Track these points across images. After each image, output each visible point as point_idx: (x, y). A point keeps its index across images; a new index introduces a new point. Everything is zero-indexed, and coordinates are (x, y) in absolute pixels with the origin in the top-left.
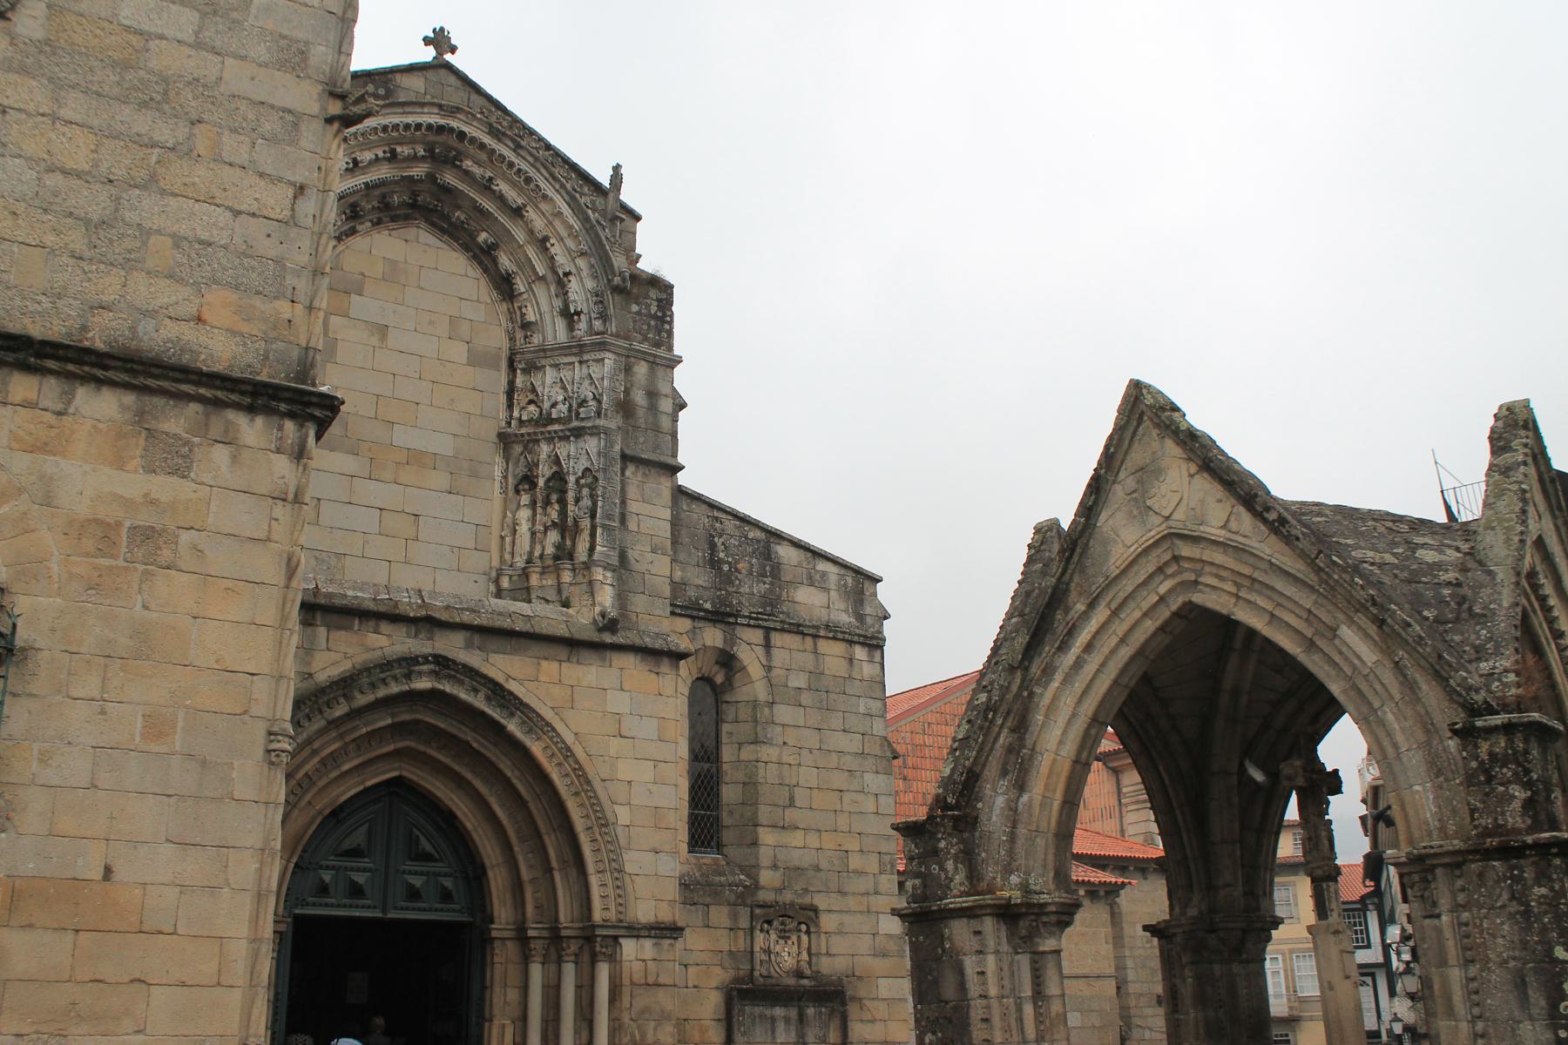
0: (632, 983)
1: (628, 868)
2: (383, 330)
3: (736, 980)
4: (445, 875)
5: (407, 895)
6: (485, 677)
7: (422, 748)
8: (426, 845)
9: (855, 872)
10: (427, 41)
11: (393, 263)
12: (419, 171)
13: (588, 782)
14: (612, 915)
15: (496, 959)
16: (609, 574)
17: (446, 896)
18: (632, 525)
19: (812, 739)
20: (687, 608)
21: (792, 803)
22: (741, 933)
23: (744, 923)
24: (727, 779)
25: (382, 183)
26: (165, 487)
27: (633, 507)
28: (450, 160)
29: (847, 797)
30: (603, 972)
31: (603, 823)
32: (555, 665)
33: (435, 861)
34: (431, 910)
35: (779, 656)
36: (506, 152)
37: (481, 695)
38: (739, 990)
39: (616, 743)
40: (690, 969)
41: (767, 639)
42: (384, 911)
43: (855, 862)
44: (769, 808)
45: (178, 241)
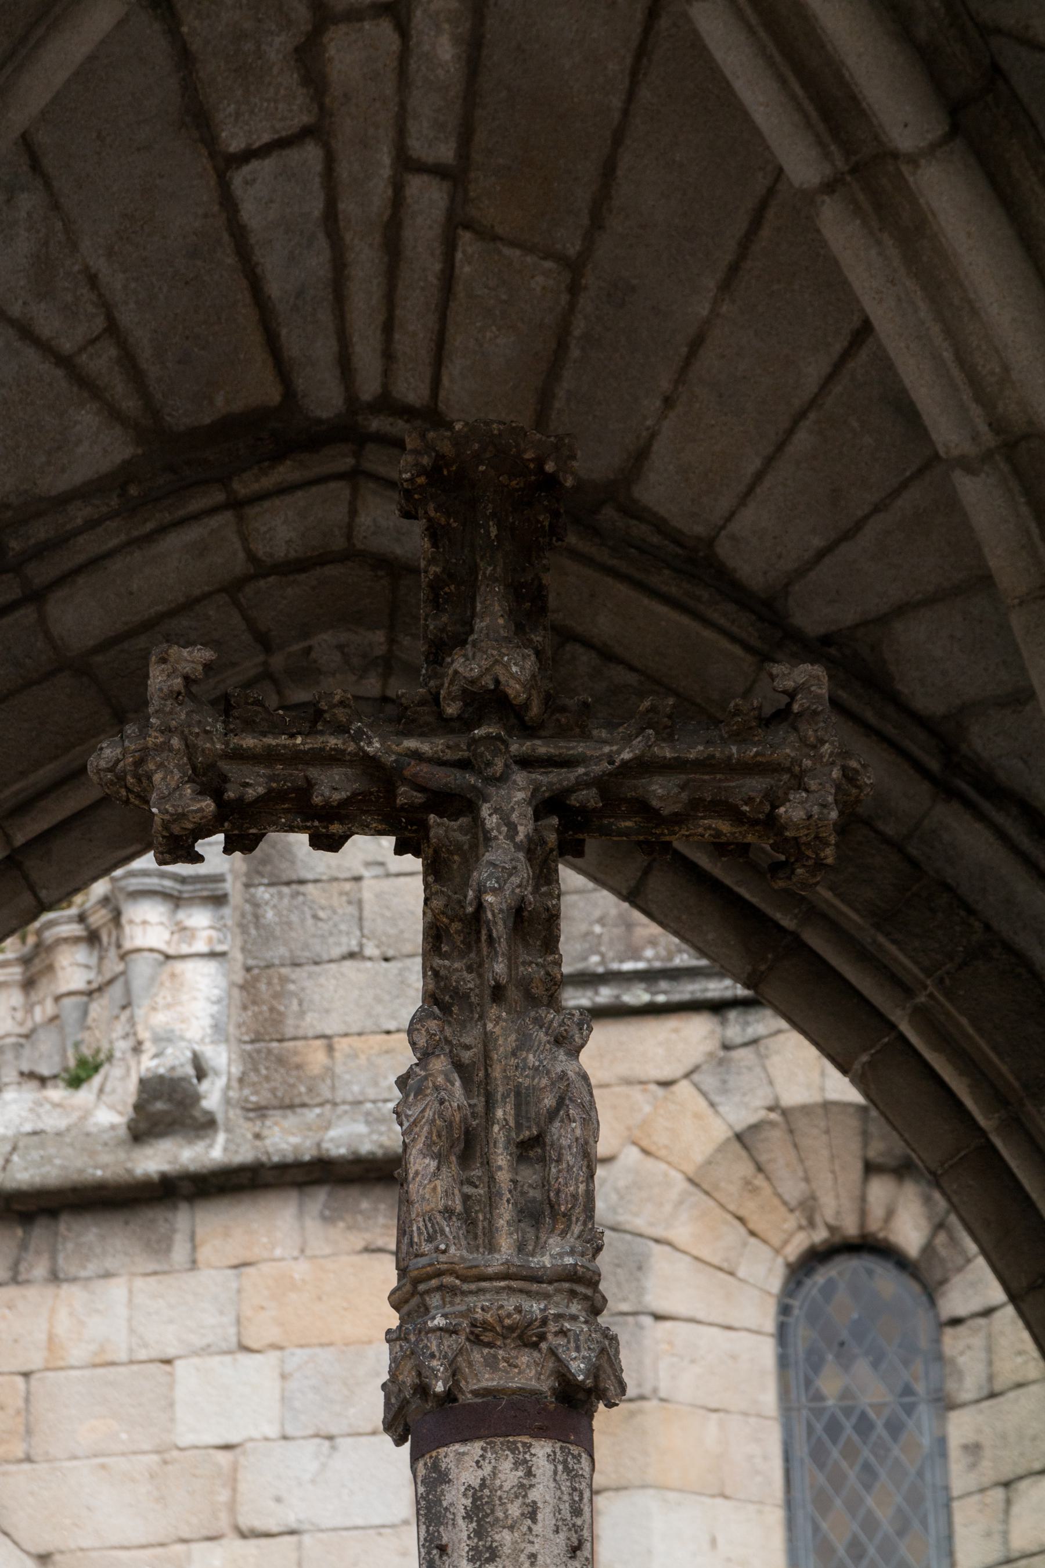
16: (199, 919)
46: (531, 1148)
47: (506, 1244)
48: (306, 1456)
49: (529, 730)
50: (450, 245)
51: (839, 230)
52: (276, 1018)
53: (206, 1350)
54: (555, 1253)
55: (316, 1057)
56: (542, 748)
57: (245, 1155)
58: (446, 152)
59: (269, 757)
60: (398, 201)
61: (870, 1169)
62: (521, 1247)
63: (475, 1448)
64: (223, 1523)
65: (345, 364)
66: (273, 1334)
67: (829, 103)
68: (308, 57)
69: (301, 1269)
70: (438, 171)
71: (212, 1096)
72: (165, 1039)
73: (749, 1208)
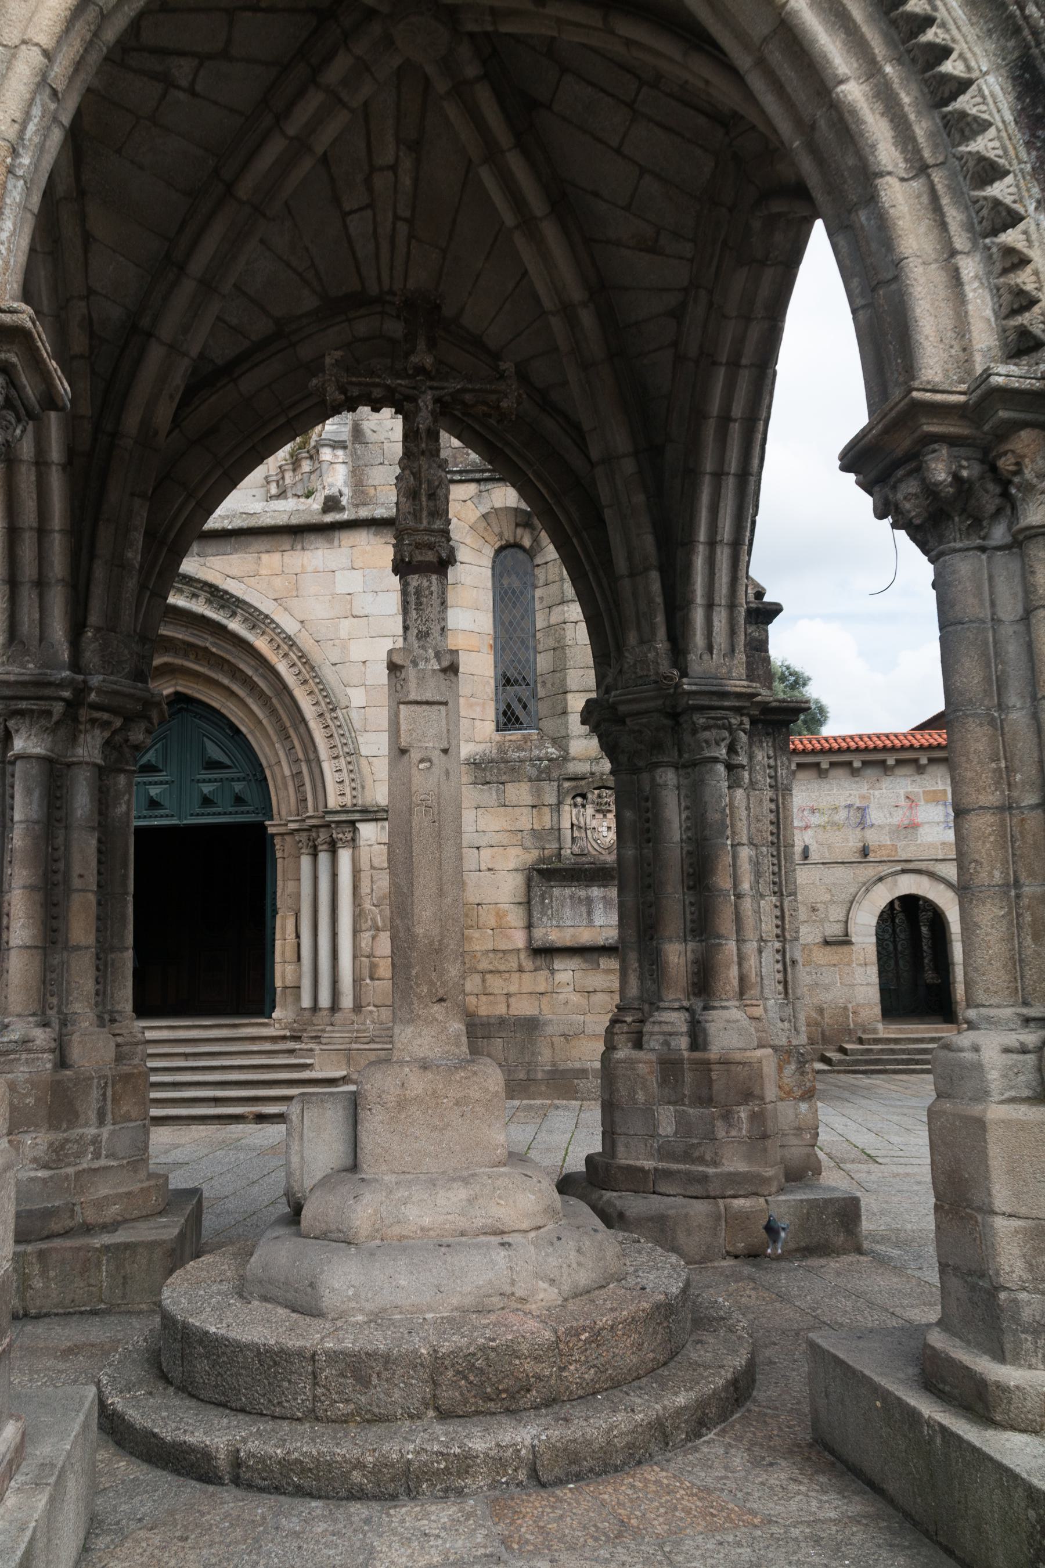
0: (372, 867)
1: (364, 751)
3: (542, 860)
4: (239, 780)
5: (174, 799)
6: (198, 581)
7: (178, 661)
8: (215, 752)
13: (313, 668)
14: (348, 800)
15: (278, 854)
16: (340, 452)
17: (239, 800)
20: (467, 472)
22: (547, 810)
23: (551, 798)
24: (540, 648)
30: (345, 856)
31: (331, 706)
32: (276, 557)
33: (229, 767)
34: (225, 814)
37: (202, 600)
38: (540, 871)
39: (346, 625)
40: (482, 851)
42: (180, 819)
44: (581, 672)
46: (432, 496)
47: (425, 522)
48: (370, 597)
49: (432, 379)
50: (409, 244)
51: (519, 241)
52: (361, 481)
53: (343, 569)
54: (438, 525)
55: (372, 491)
56: (435, 384)
57: (353, 517)
58: (407, 214)
59: (359, 384)
60: (394, 229)
61: (517, 525)
62: (429, 523)
63: (417, 576)
64: (349, 614)
65: (379, 278)
66: (361, 565)
67: (518, 202)
68: (368, 181)
69: (368, 548)
70: (405, 220)
71: (344, 501)
72: (331, 485)
73: (485, 535)
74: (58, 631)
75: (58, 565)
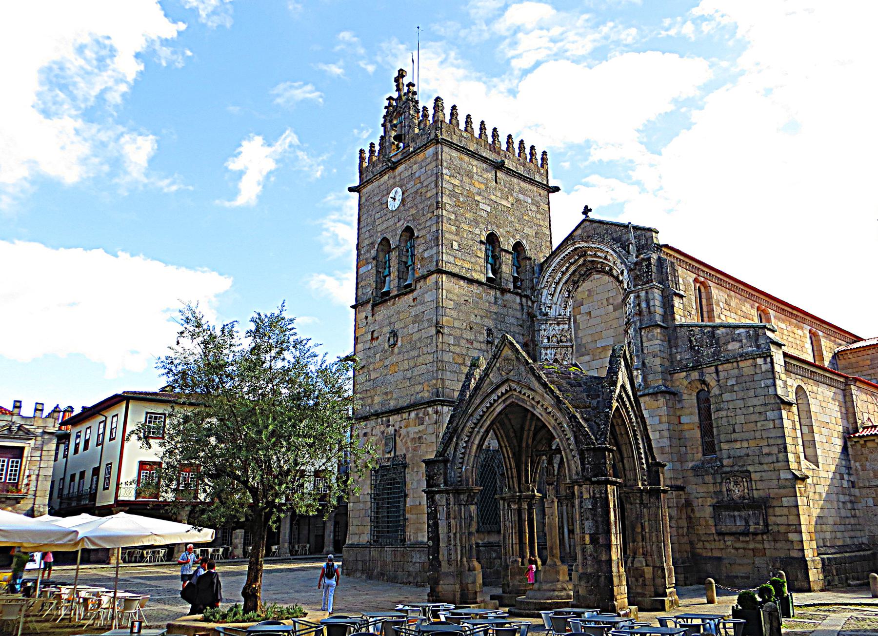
2: (589, 313)
9: (766, 454)
10: (583, 213)
11: (589, 290)
12: (581, 261)
18: (645, 352)
19: (740, 404)
21: (734, 431)
23: (719, 480)
25: (575, 271)
26: (421, 428)
27: (645, 345)
28: (585, 255)
29: (759, 424)
35: (722, 375)
36: (592, 245)
41: (717, 369)
43: (765, 450)
45: (420, 375)
74: (516, 486)
75: (515, 474)
